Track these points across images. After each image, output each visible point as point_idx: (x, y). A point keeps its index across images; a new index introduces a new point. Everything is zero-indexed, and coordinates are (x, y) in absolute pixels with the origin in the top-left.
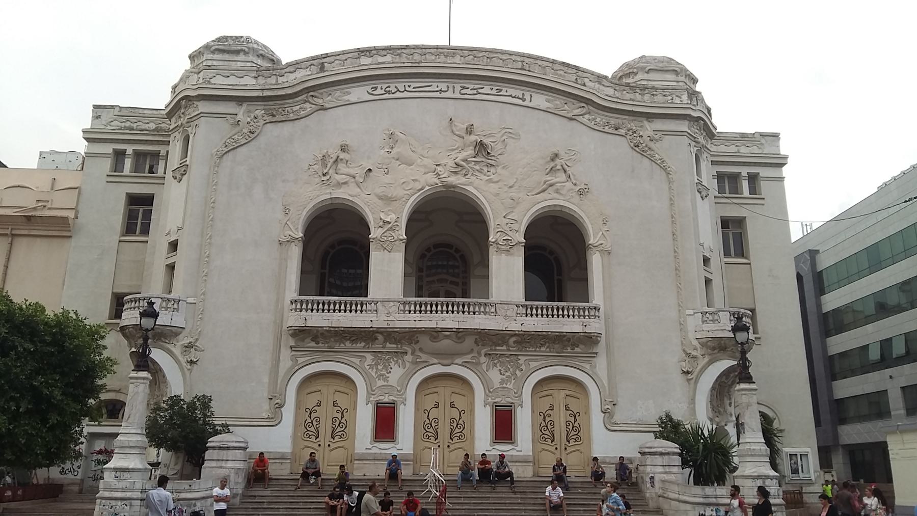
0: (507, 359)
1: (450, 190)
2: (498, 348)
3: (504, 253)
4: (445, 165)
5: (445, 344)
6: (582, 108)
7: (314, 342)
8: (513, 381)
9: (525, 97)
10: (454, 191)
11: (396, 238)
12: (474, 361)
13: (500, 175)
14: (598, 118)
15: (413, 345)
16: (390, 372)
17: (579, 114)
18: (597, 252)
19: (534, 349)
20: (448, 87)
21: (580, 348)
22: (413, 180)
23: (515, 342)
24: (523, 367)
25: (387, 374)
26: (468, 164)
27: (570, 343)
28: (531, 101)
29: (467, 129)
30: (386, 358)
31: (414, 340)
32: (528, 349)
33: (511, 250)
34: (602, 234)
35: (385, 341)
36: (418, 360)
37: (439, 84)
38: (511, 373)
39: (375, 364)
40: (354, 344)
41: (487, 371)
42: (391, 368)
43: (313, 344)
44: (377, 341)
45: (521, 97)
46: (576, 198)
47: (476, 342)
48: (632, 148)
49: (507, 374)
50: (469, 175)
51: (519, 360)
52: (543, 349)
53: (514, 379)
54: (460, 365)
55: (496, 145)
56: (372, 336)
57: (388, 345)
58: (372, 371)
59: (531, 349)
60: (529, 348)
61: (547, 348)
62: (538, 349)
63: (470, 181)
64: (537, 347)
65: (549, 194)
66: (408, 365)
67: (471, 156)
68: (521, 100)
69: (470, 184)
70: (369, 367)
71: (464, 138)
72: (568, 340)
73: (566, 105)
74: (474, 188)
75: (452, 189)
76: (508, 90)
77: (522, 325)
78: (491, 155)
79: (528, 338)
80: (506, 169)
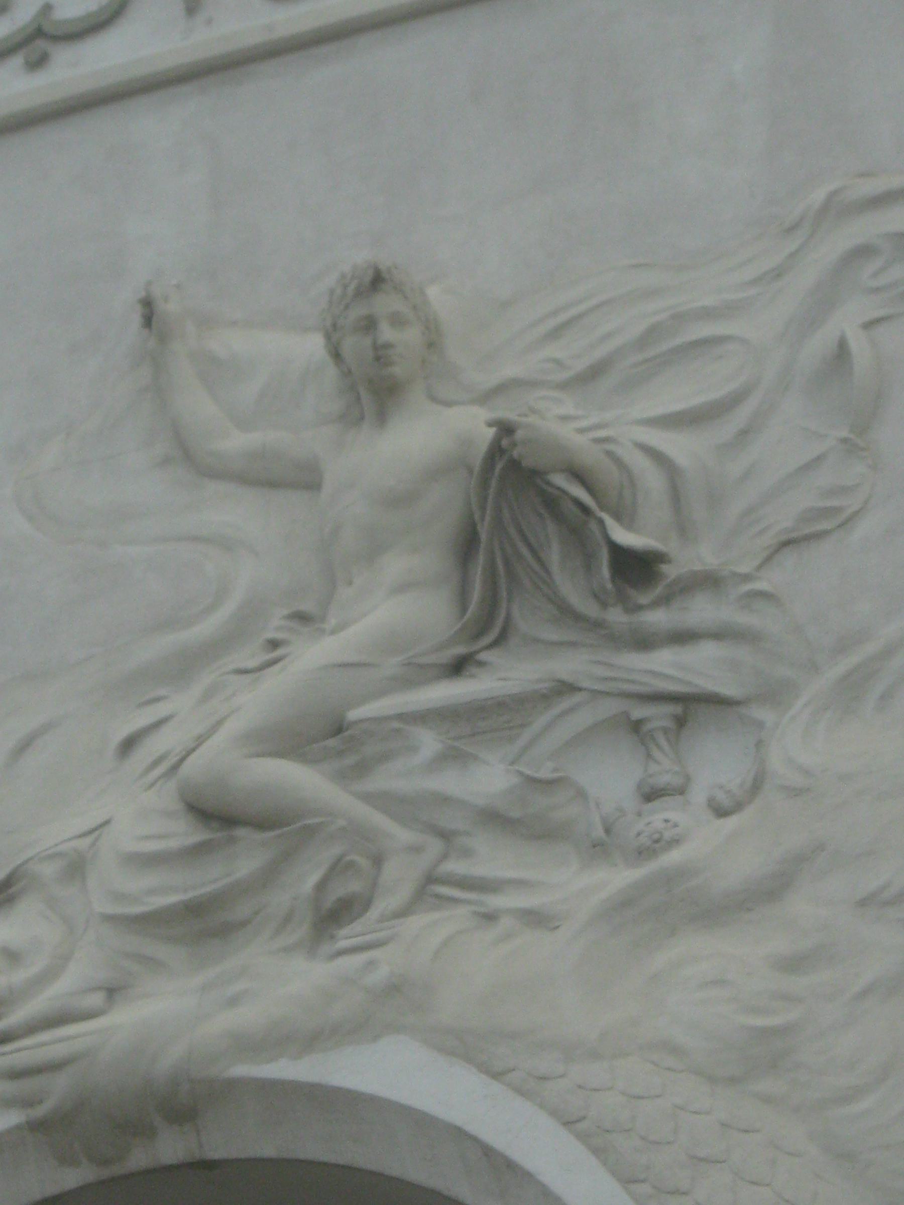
10: (208, 1165)
13: (794, 792)
26: (363, 769)
29: (336, 355)
50: (383, 905)
55: (745, 434)
63: (379, 976)
67: (391, 666)
78: (670, 571)
80: (886, 697)
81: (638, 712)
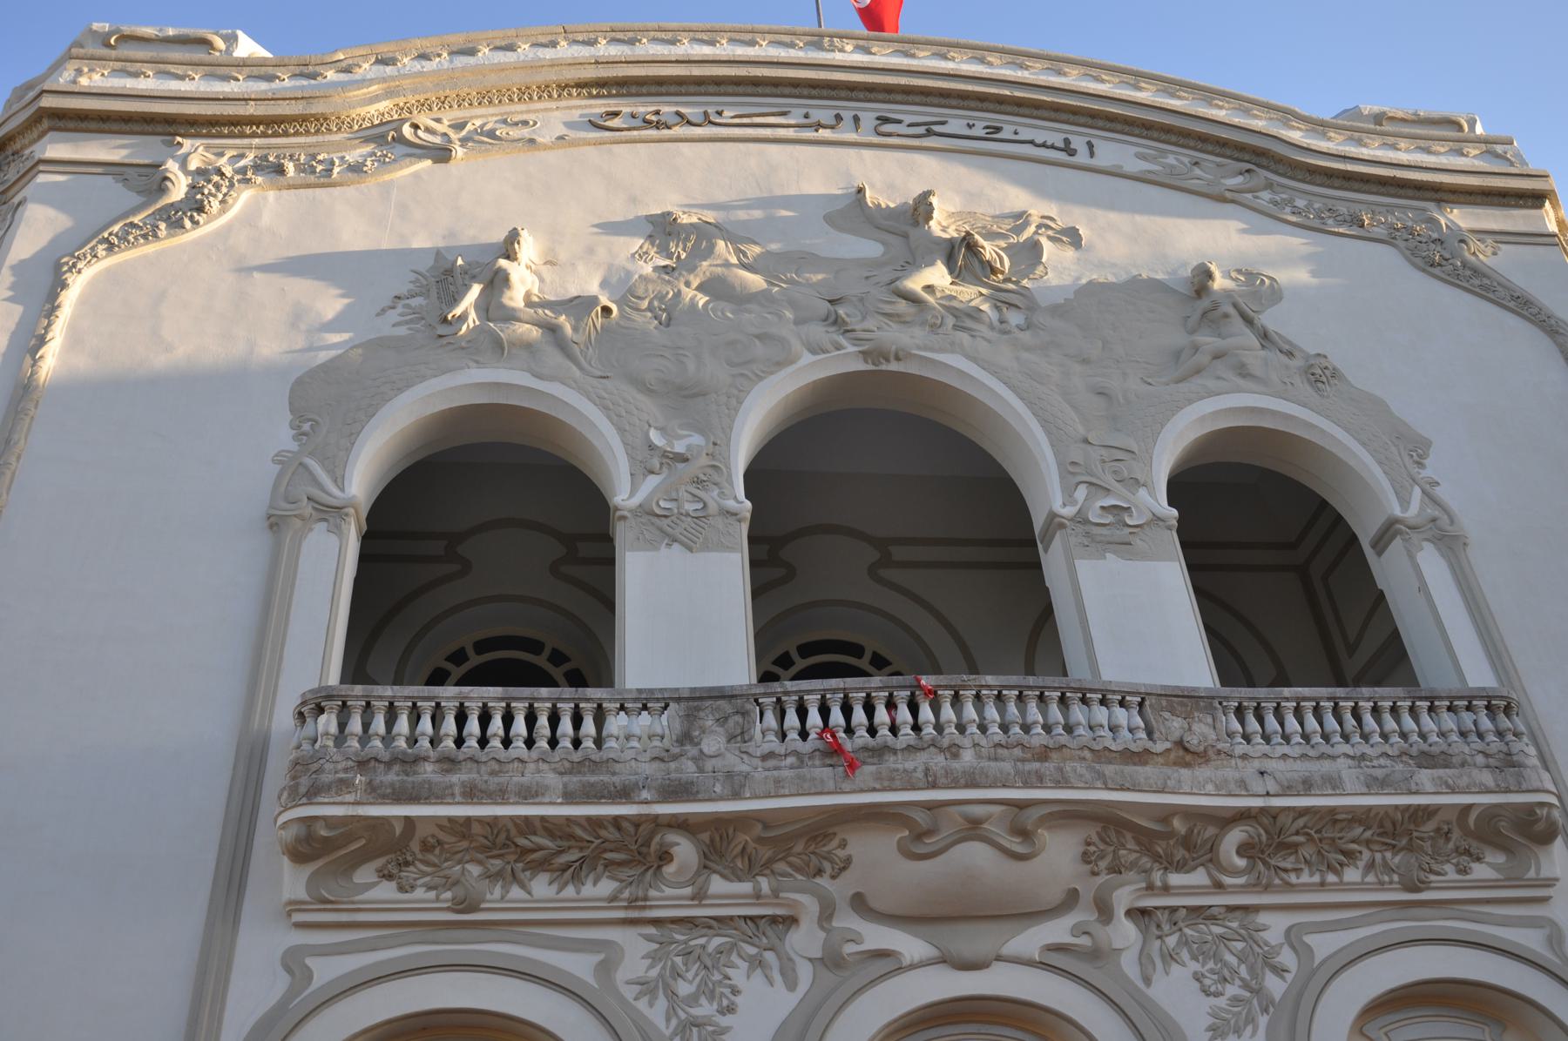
0: (1217, 930)
1: (884, 367)
2: (1175, 879)
3: (1115, 552)
4: (861, 300)
5: (976, 855)
6: (1246, 174)
7: (393, 884)
8: (1263, 1021)
9: (1072, 146)
11: (713, 508)
12: (1084, 941)
14: (1297, 200)
15: (824, 881)
16: (730, 1009)
17: (1247, 186)
18: (1425, 544)
19: (1316, 879)
20: (839, 118)
21: (1488, 864)
22: (758, 337)
23: (1242, 850)
24: (1287, 958)
25: (724, 1021)
27: (1451, 845)
28: (1092, 154)
30: (712, 946)
31: (828, 857)
32: (1293, 878)
33: (1137, 541)
34: (1424, 492)
35: (705, 867)
36: (850, 948)
37: (811, 111)
38: (1245, 985)
39: (661, 975)
40: (566, 884)
41: (1147, 981)
42: (735, 991)
43: (386, 891)
44: (669, 869)
45: (1061, 145)
46: (1305, 389)
47: (1086, 858)
48: (1424, 270)
49: (1232, 990)
51: (1265, 928)
52: (1352, 875)
53: (1265, 1010)
54: (1030, 963)
56: (647, 843)
57: (718, 885)
58: (651, 1005)
59: (1305, 878)
60: (1298, 871)
61: (1371, 866)
62: (1331, 878)
64: (1330, 867)
65: (1219, 378)
66: (805, 973)
68: (1064, 153)
69: (953, 348)
70: (638, 988)
71: (905, 236)
72: (1446, 828)
73: (1197, 172)
74: (968, 357)
75: (894, 366)
76: (1020, 129)
77: (1262, 773)
79: (1301, 822)
81: (999, 304)
